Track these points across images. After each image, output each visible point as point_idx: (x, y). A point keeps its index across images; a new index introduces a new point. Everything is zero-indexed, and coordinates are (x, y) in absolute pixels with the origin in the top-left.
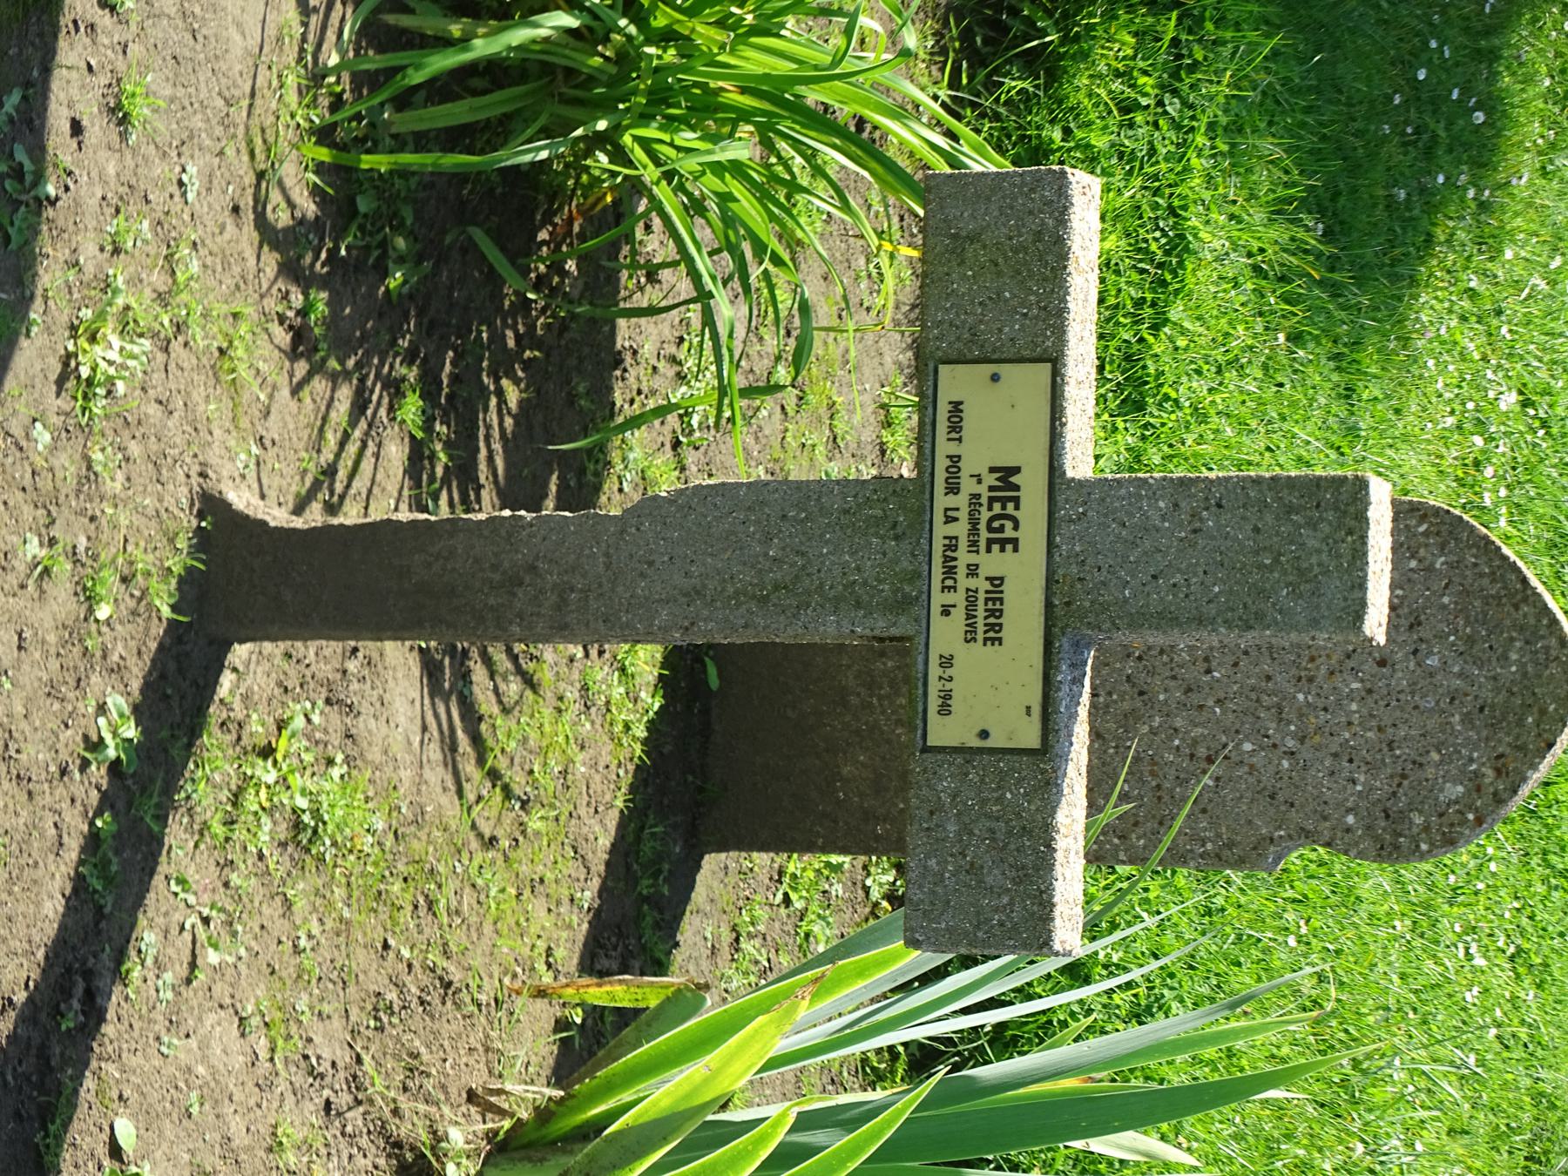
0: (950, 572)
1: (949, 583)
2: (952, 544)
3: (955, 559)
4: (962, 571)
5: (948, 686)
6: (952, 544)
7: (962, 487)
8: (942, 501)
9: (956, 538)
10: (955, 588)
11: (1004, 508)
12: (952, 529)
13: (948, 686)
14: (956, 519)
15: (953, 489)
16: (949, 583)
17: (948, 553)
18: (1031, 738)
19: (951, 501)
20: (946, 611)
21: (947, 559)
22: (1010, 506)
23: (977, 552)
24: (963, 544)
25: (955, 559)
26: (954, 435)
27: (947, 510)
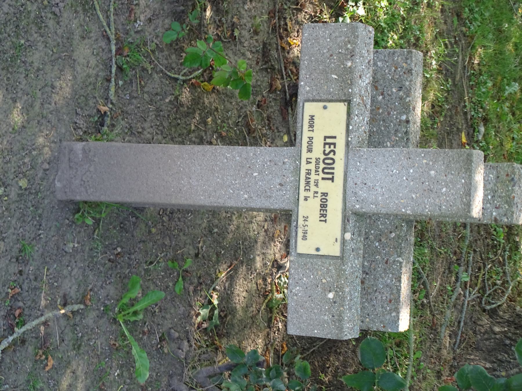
0: (308, 183)
1: (307, 188)
2: (309, 172)
3: (309, 178)
4: (312, 183)
5: (306, 228)
6: (309, 172)
7: (313, 150)
8: (305, 155)
9: (311, 170)
10: (309, 190)
12: (310, 166)
13: (306, 228)
14: (310, 163)
15: (310, 150)
16: (307, 188)
17: (308, 176)
18: (338, 253)
19: (309, 155)
20: (306, 199)
21: (307, 178)
23: (318, 174)
24: (313, 172)
25: (309, 178)
26: (311, 129)
27: (307, 159)
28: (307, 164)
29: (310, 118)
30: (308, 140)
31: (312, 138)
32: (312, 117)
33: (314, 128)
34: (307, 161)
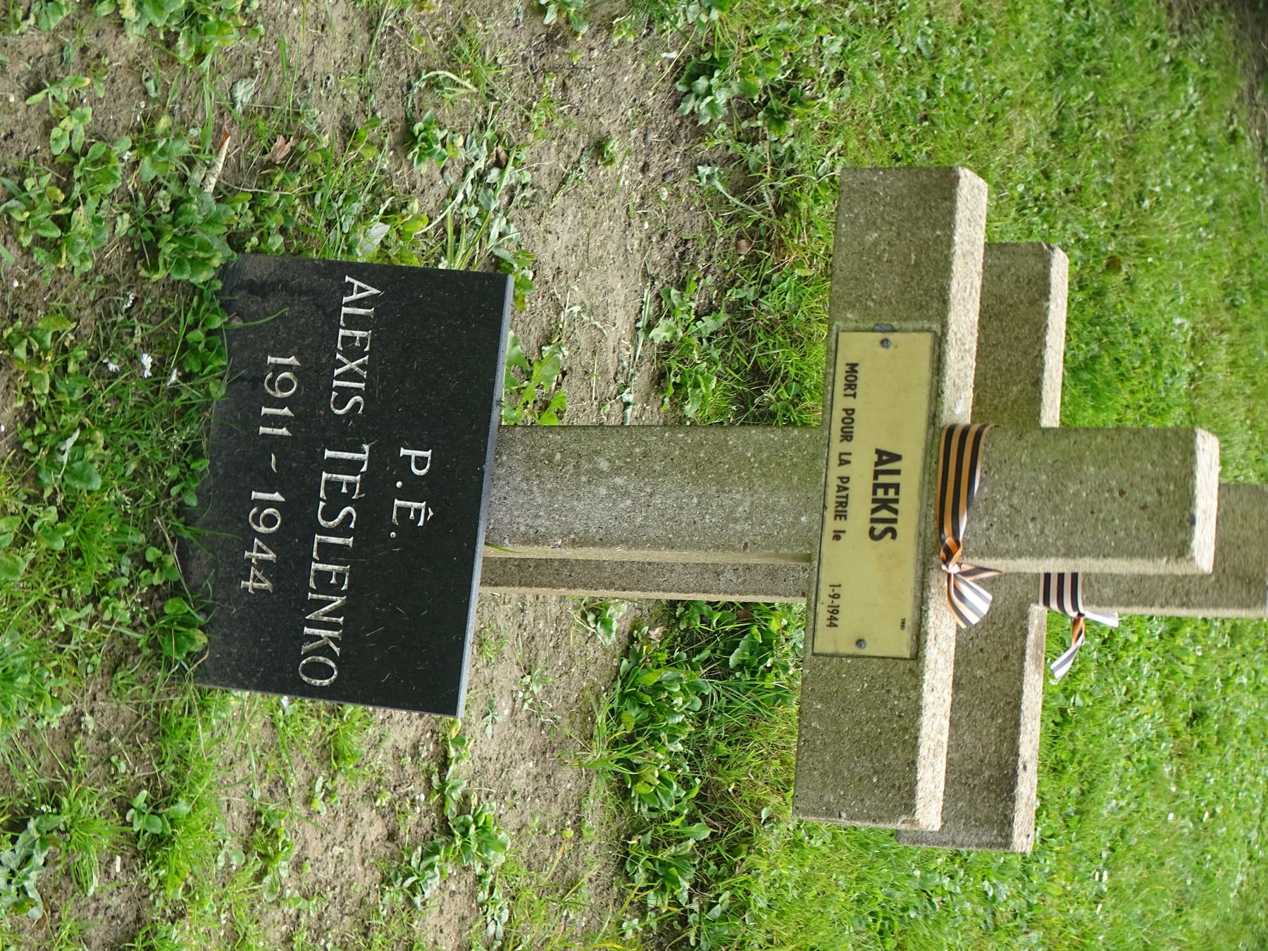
0: (843, 504)
8: (837, 446)
11: (886, 493)
12: (844, 471)
14: (848, 462)
15: (847, 436)
18: (906, 653)
19: (846, 446)
22: (891, 492)
26: (849, 392)
27: (841, 454)
28: (841, 464)
29: (847, 368)
30: (844, 415)
31: (853, 410)
32: (853, 368)
33: (858, 390)
34: (841, 460)
